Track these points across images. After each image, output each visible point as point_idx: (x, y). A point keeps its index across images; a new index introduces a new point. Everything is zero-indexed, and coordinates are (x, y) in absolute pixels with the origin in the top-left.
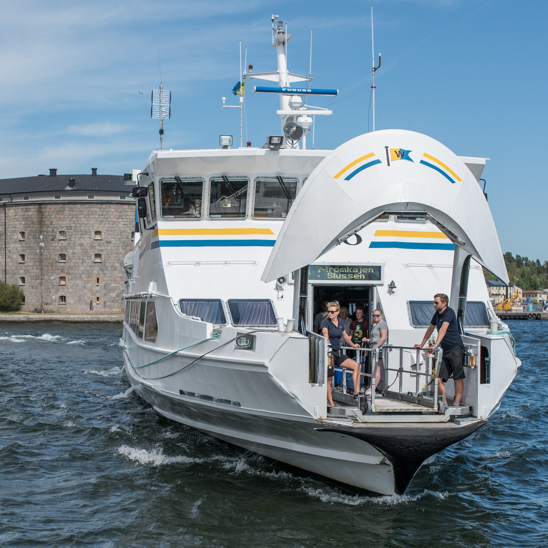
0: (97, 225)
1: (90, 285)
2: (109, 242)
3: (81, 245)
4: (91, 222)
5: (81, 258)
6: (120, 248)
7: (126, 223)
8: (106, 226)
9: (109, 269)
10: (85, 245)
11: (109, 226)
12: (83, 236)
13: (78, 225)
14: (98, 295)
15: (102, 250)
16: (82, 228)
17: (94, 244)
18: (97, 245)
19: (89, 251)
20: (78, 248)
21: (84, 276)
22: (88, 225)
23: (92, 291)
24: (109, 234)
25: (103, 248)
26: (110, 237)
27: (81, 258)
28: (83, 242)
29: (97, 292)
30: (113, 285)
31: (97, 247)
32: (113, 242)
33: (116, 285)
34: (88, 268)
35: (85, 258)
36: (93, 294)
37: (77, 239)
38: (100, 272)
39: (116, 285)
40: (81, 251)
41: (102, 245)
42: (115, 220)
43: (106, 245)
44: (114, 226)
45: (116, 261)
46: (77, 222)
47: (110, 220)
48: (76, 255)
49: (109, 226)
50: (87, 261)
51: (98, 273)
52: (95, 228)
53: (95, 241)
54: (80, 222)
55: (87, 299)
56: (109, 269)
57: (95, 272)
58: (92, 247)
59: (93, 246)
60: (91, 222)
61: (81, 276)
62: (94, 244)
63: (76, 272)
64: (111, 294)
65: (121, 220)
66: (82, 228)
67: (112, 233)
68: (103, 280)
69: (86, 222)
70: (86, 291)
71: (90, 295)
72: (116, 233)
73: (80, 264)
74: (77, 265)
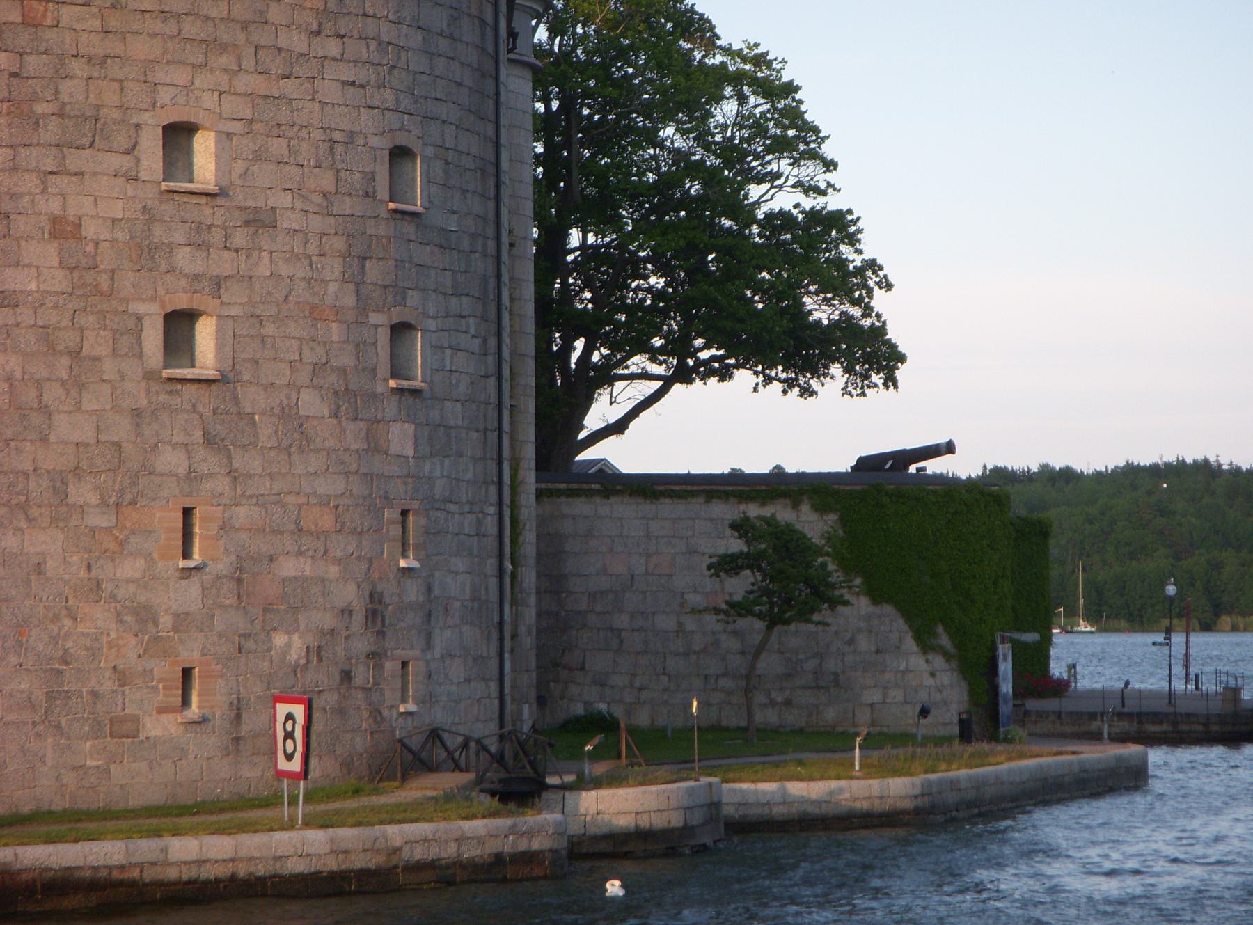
0: (180, 76)
1: (130, 568)
2: (260, 221)
3: (63, 230)
4: (141, 48)
5: (67, 339)
6: (333, 269)
7: (362, 74)
8: (246, 82)
9: (266, 433)
10: (90, 229)
11: (258, 84)
12: (76, 160)
13: (34, 63)
14: (190, 653)
15: (218, 283)
16: (66, 87)
17: (158, 233)
18: (179, 235)
19: (127, 281)
20: (45, 254)
21: (83, 493)
22: (115, 70)
23: (145, 615)
24: (259, 156)
25: (222, 263)
26: (264, 174)
27: (67, 339)
28: (80, 205)
29: (182, 621)
30: (288, 567)
31: (185, 259)
32: (283, 223)
33: (306, 567)
34: (121, 429)
35: (96, 344)
36: (156, 646)
37: (30, 182)
38: (208, 462)
39: (306, 567)
40: (59, 281)
41: (217, 236)
42: (298, 42)
43: (240, 238)
44: (289, 88)
45: (304, 376)
46: (23, 39)
47: (262, 36)
48: (25, 316)
49: (258, 84)
50: (109, 368)
51: (192, 476)
52: (165, 95)
53: (167, 209)
54: (50, 35)
55: (108, 685)
56: (266, 433)
57: (171, 460)
58: (147, 253)
59: (152, 249)
60: (141, 48)
61: (61, 494)
62: (158, 233)
63: (28, 466)
64: (279, 640)
65: (333, 48)
66: (66, 87)
67: (278, 147)
68: (226, 527)
69: (95, 45)
70: (99, 617)
71: (131, 649)
72: (306, 152)
73: (53, 394)
74: (29, 396)
